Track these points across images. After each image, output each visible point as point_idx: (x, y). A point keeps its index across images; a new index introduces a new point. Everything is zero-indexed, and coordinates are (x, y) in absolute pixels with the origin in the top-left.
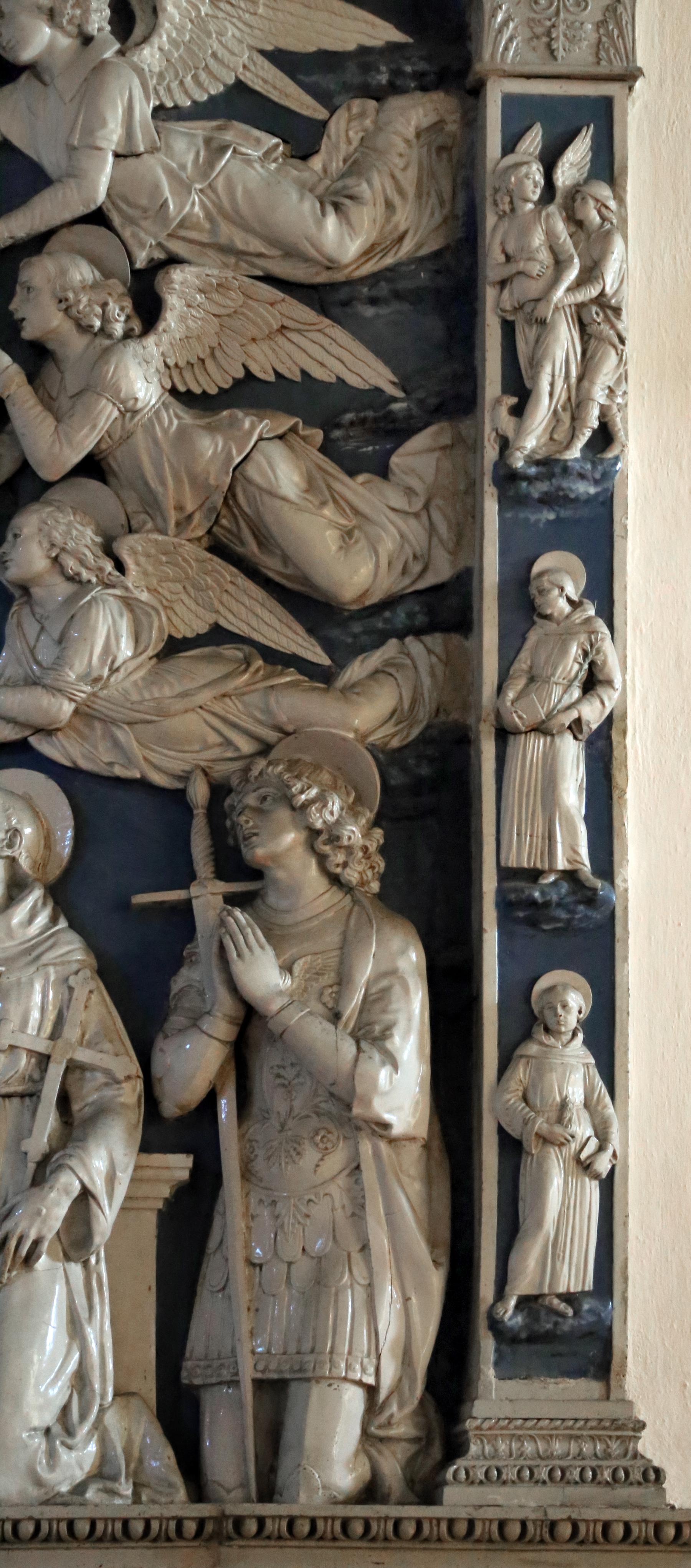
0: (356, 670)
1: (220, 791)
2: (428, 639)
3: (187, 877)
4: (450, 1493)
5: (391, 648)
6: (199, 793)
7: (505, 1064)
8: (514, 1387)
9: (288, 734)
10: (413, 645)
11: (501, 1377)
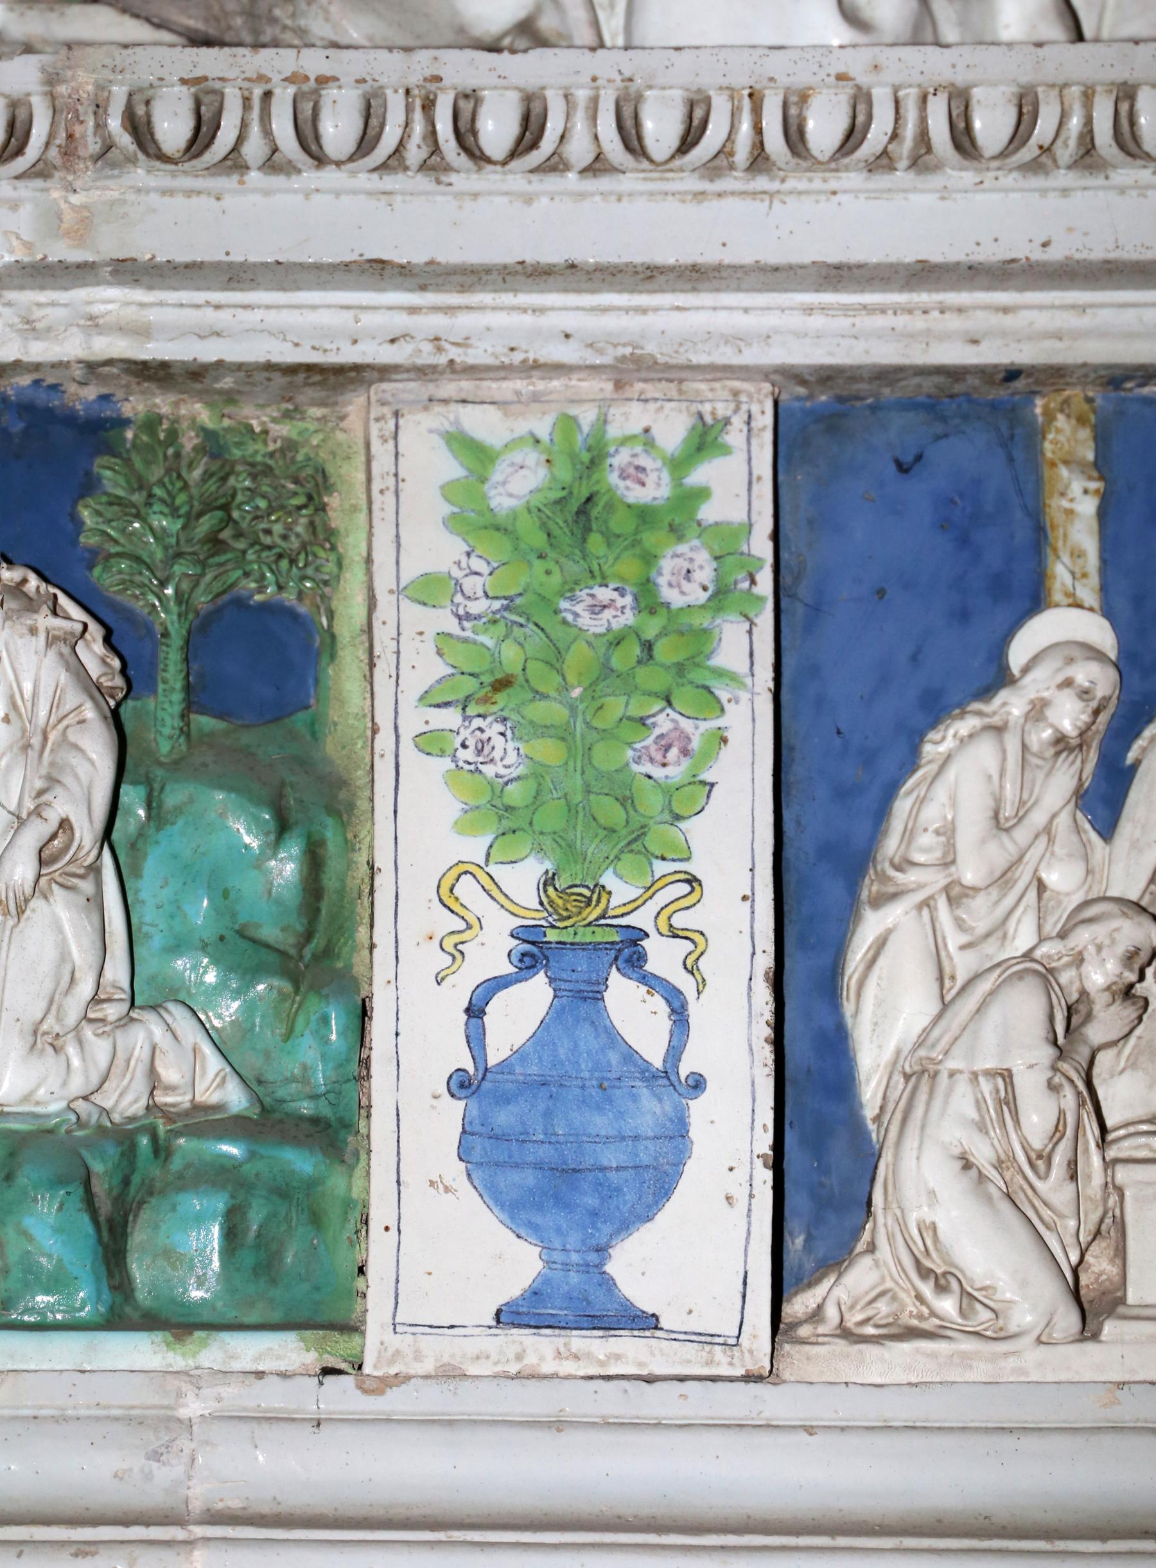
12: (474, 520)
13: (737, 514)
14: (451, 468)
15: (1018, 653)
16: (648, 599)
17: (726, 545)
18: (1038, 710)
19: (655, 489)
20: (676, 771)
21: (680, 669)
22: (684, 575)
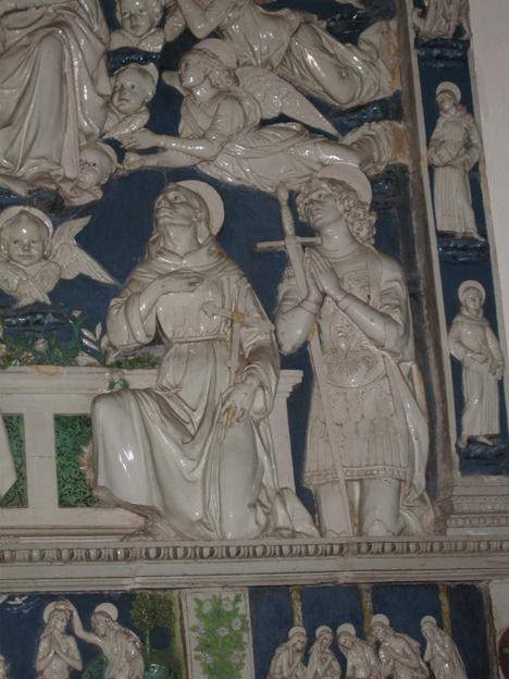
0: (350, 138)
1: (293, 195)
2: (382, 123)
3: (282, 235)
4: (450, 532)
5: (364, 129)
6: (283, 196)
7: (449, 324)
8: (470, 480)
9: (325, 166)
10: (377, 127)
11: (463, 474)
12: (200, 615)
13: (244, 612)
14: (195, 605)
15: (290, 634)
16: (230, 629)
17: (243, 618)
18: (294, 644)
19: (230, 609)
20: (237, 661)
21: (237, 642)
22: (237, 624)
